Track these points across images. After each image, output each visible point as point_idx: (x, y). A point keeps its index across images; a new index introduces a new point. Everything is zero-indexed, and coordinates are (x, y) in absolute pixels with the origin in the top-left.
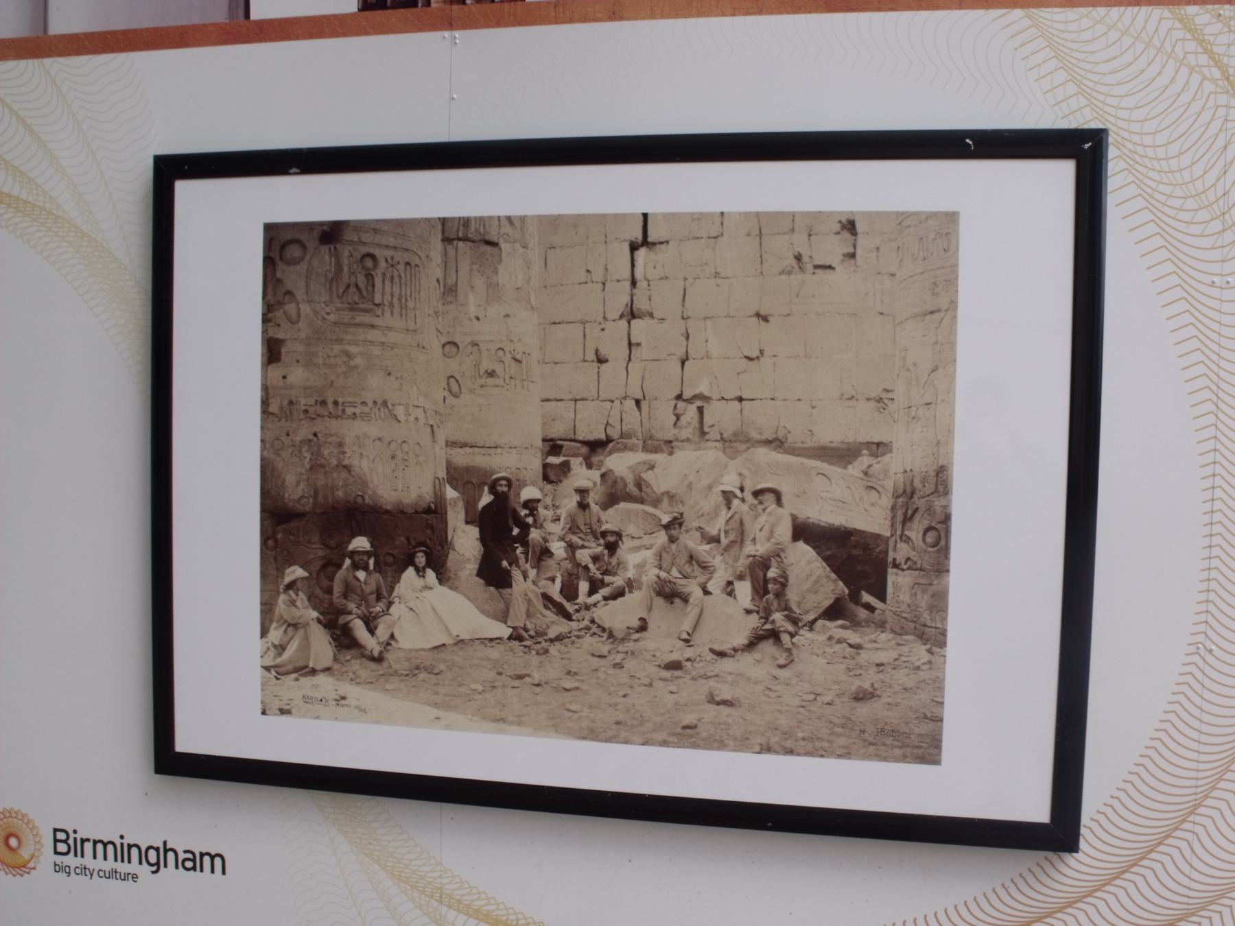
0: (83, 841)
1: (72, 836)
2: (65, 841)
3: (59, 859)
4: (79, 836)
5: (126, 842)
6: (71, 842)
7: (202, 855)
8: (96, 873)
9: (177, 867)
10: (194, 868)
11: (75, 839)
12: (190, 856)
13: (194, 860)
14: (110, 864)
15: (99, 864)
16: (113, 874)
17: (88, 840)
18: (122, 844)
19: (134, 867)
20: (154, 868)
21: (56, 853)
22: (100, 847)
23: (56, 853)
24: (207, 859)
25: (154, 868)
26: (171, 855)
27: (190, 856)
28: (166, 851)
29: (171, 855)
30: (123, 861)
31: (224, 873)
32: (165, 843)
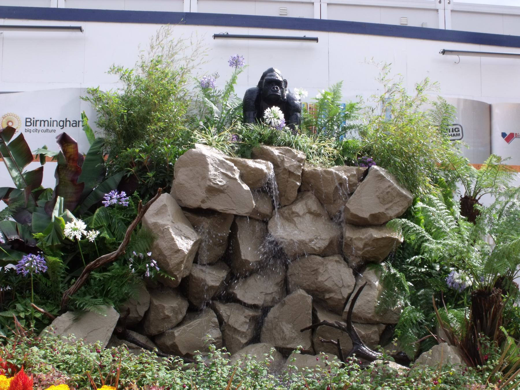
0: (36, 121)
1: (32, 120)
2: (30, 122)
3: (27, 128)
4: (35, 120)
5: (52, 120)
6: (32, 122)
8: (40, 131)
10: (76, 126)
11: (34, 121)
12: (75, 122)
13: (76, 124)
14: (46, 127)
15: (42, 128)
16: (47, 131)
19: (55, 128)
20: (62, 127)
21: (26, 126)
22: (43, 122)
23: (26, 126)
26: (68, 123)
28: (66, 121)
30: (51, 126)
32: (66, 119)
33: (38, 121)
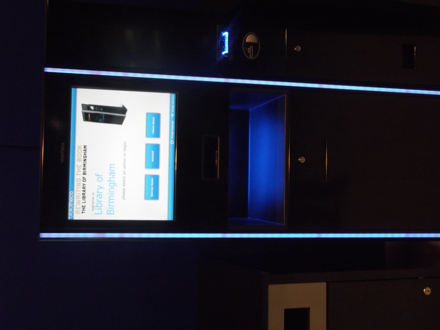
0: (110, 206)
1: (108, 209)
2: (110, 211)
6: (110, 210)
7: (111, 170)
9: (114, 178)
11: (109, 208)
12: (111, 174)
17: (109, 204)
18: (110, 194)
22: (111, 201)
24: (112, 169)
25: (115, 185)
26: (111, 179)
27: (111, 174)
28: (110, 181)
29: (111, 179)
31: (114, 164)
32: (108, 181)
33: (109, 204)
